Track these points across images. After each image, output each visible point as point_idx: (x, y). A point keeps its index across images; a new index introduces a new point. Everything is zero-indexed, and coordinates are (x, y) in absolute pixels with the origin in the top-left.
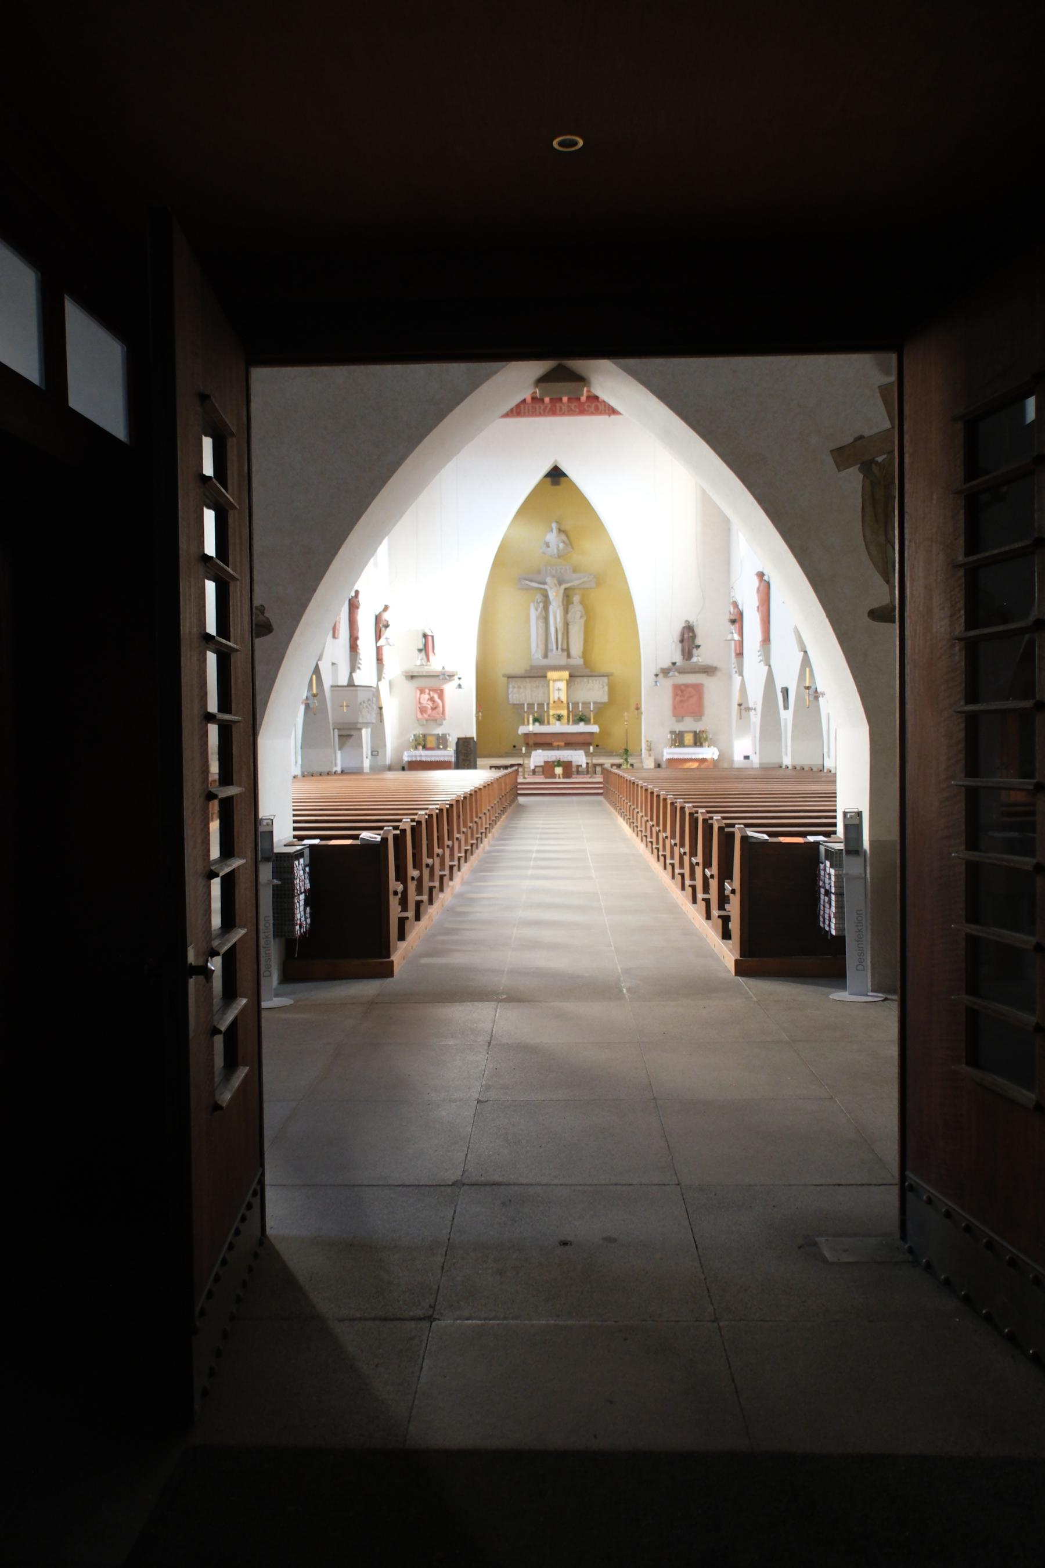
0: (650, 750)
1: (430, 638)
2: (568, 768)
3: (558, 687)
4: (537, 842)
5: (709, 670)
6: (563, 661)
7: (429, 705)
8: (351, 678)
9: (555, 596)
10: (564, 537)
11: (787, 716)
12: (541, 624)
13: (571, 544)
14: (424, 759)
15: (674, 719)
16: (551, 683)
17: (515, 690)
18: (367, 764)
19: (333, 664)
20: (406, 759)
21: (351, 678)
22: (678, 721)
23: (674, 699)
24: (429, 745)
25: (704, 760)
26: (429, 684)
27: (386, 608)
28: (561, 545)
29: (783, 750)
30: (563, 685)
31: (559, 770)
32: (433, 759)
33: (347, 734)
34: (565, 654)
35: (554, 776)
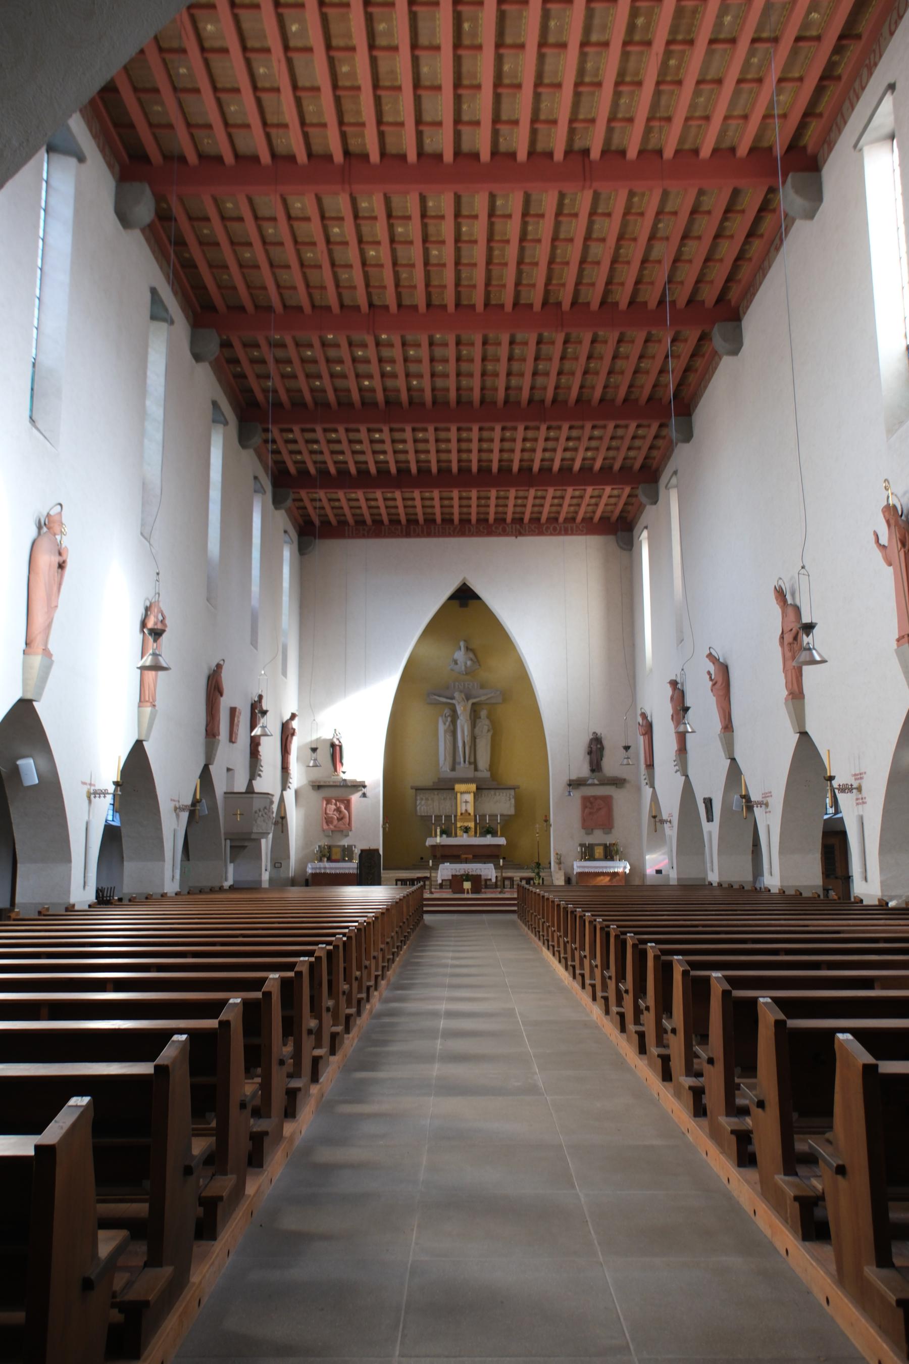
0: (560, 863)
1: (338, 748)
2: (478, 882)
3: (465, 799)
4: (446, 993)
5: (618, 782)
6: (471, 774)
7: (336, 816)
8: (250, 785)
9: (463, 710)
10: (471, 655)
11: (711, 830)
12: (449, 737)
13: (478, 661)
14: (328, 871)
15: (583, 831)
16: (459, 795)
17: (423, 802)
18: (265, 876)
19: (228, 770)
20: (309, 871)
21: (250, 785)
22: (588, 834)
23: (583, 811)
24: (334, 857)
25: (615, 874)
26: (334, 792)
27: (293, 716)
28: (469, 663)
29: (709, 865)
30: (470, 798)
31: (467, 885)
32: (338, 871)
33: (242, 845)
34: (473, 766)
35: (462, 891)
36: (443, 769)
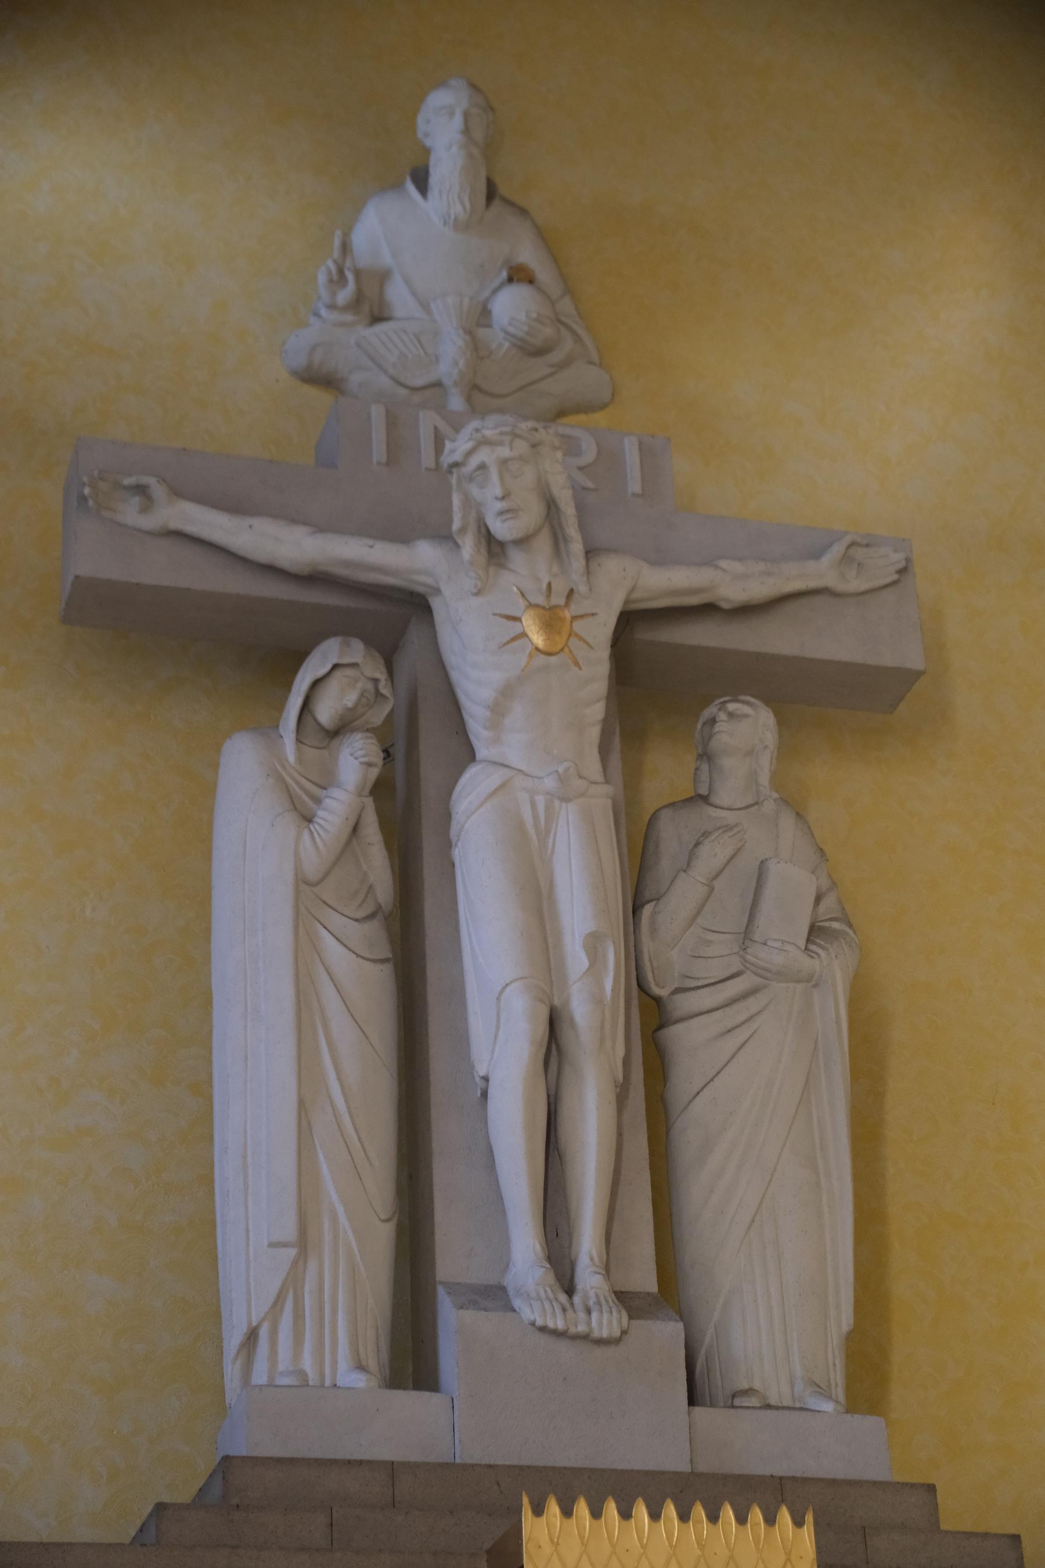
9: (519, 664)
12: (354, 972)
36: (281, 1358)
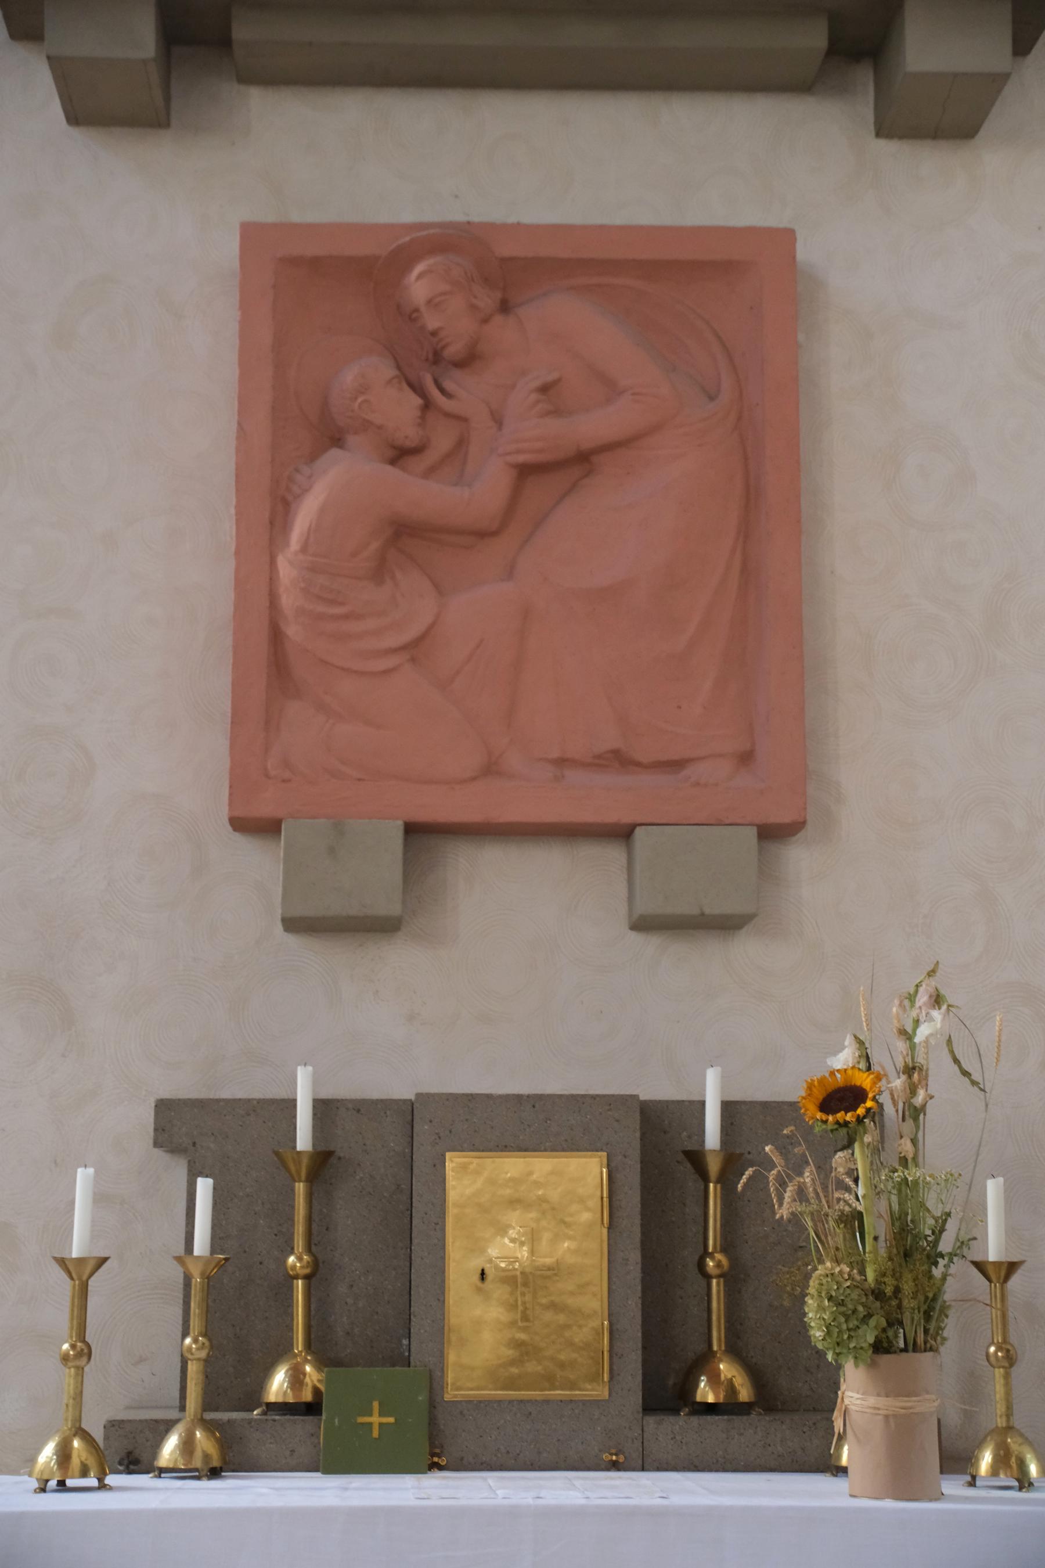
23: (268, 506)
